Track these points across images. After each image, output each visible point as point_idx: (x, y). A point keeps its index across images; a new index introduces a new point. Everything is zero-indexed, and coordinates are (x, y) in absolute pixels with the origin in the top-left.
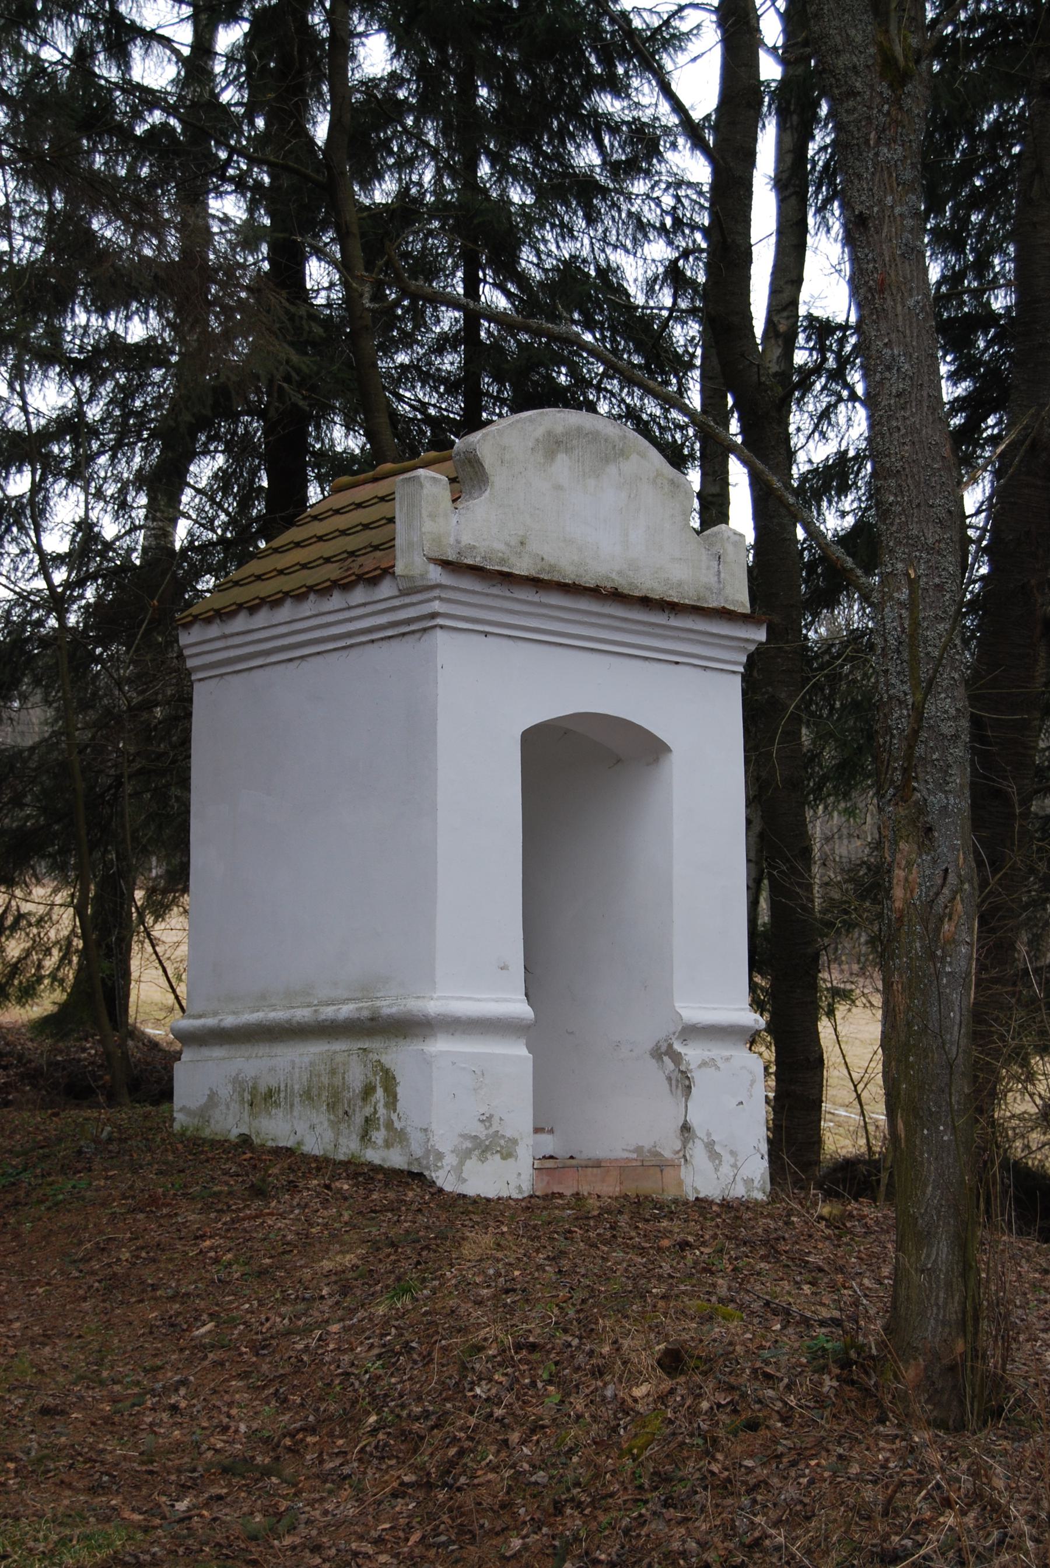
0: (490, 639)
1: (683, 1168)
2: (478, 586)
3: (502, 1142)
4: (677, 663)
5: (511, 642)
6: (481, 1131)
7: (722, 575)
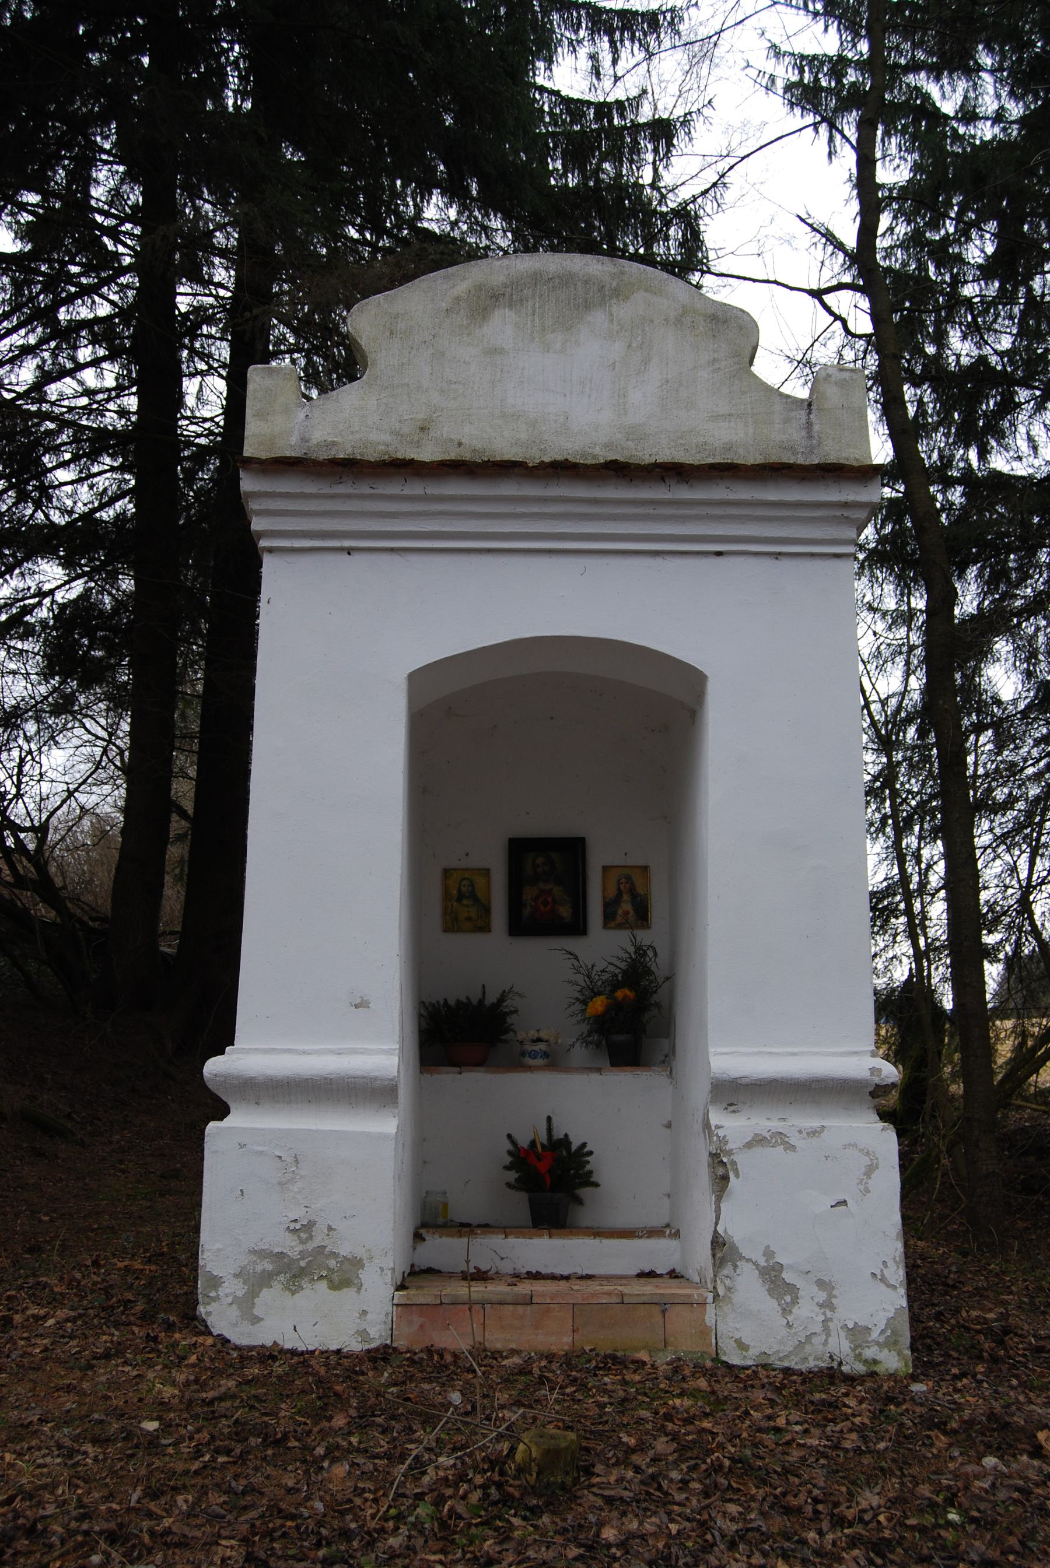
0: (356, 557)
1: (710, 1309)
2: (310, 487)
3: (332, 1263)
4: (719, 554)
5: (396, 558)
6: (291, 1246)
7: (816, 428)
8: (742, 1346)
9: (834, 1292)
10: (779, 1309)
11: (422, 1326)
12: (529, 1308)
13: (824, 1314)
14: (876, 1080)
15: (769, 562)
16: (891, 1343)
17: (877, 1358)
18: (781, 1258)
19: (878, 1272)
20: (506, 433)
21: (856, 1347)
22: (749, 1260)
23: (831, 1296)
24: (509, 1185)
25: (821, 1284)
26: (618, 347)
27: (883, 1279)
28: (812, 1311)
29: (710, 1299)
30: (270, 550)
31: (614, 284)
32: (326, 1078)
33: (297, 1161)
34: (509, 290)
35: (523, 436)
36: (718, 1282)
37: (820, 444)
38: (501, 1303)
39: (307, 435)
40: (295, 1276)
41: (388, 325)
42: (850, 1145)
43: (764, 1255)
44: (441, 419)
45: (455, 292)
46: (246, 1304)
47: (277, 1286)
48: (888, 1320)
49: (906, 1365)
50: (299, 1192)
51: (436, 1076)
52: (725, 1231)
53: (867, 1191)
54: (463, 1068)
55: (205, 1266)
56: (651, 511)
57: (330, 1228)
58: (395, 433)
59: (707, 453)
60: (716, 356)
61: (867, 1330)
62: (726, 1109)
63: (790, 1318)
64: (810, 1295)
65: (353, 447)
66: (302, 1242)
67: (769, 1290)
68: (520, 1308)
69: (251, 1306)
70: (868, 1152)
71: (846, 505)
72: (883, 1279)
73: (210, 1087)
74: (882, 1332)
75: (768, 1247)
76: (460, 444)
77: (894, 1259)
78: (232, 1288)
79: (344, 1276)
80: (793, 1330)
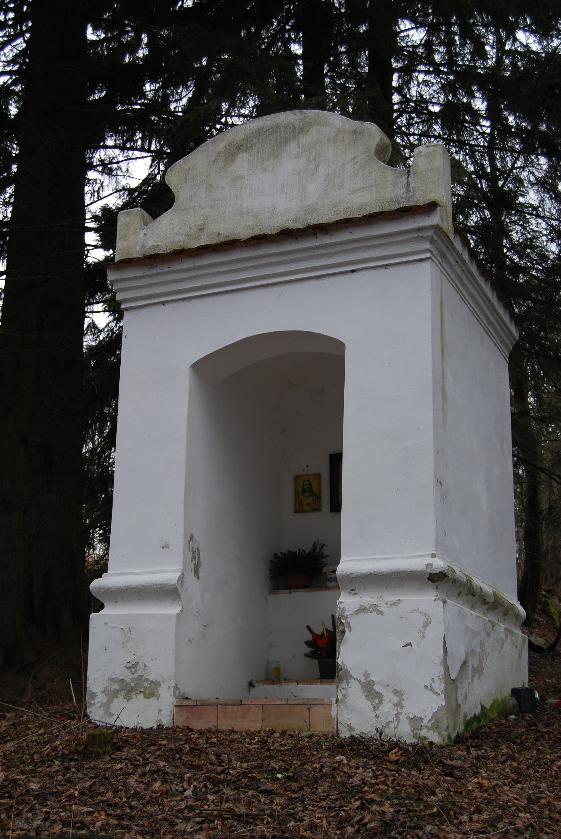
0: (167, 306)
1: (334, 707)
2: (139, 272)
3: (146, 684)
4: (353, 271)
5: (186, 303)
6: (127, 675)
7: (412, 185)
8: (350, 728)
9: (403, 697)
10: (372, 707)
11: (187, 718)
12: (240, 707)
13: (397, 710)
14: (429, 570)
15: (381, 271)
16: (435, 727)
17: (426, 736)
18: (374, 678)
19: (429, 685)
20: (242, 224)
21: (415, 729)
22: (356, 679)
23: (401, 699)
24: (306, 655)
25: (396, 692)
26: (302, 161)
27: (432, 690)
28: (390, 708)
29: (334, 702)
30: (127, 309)
31: (301, 125)
32: (143, 586)
33: (130, 631)
34: (245, 142)
35: (251, 223)
36: (339, 691)
37: (414, 194)
38: (226, 705)
39: (144, 244)
40: (129, 692)
41: (185, 175)
42: (415, 610)
43: (364, 676)
44: (210, 222)
45: (218, 150)
46: (107, 706)
47: (121, 697)
48: (434, 713)
49: (444, 740)
50: (131, 647)
51: (278, 596)
52: (342, 662)
53: (424, 637)
54: (292, 590)
55: (89, 687)
56: (312, 254)
57: (145, 666)
58: (187, 235)
59: (349, 213)
60: (355, 154)
61: (421, 719)
62: (350, 593)
63: (378, 712)
64: (389, 698)
65: (166, 246)
66: (133, 673)
67: (366, 696)
68: (236, 707)
69: (111, 707)
70: (425, 614)
71: (419, 229)
72: (432, 690)
73: (93, 594)
74: (430, 720)
75: (366, 671)
76: (219, 234)
77: (439, 677)
78: (101, 698)
79: (151, 691)
80: (379, 719)
